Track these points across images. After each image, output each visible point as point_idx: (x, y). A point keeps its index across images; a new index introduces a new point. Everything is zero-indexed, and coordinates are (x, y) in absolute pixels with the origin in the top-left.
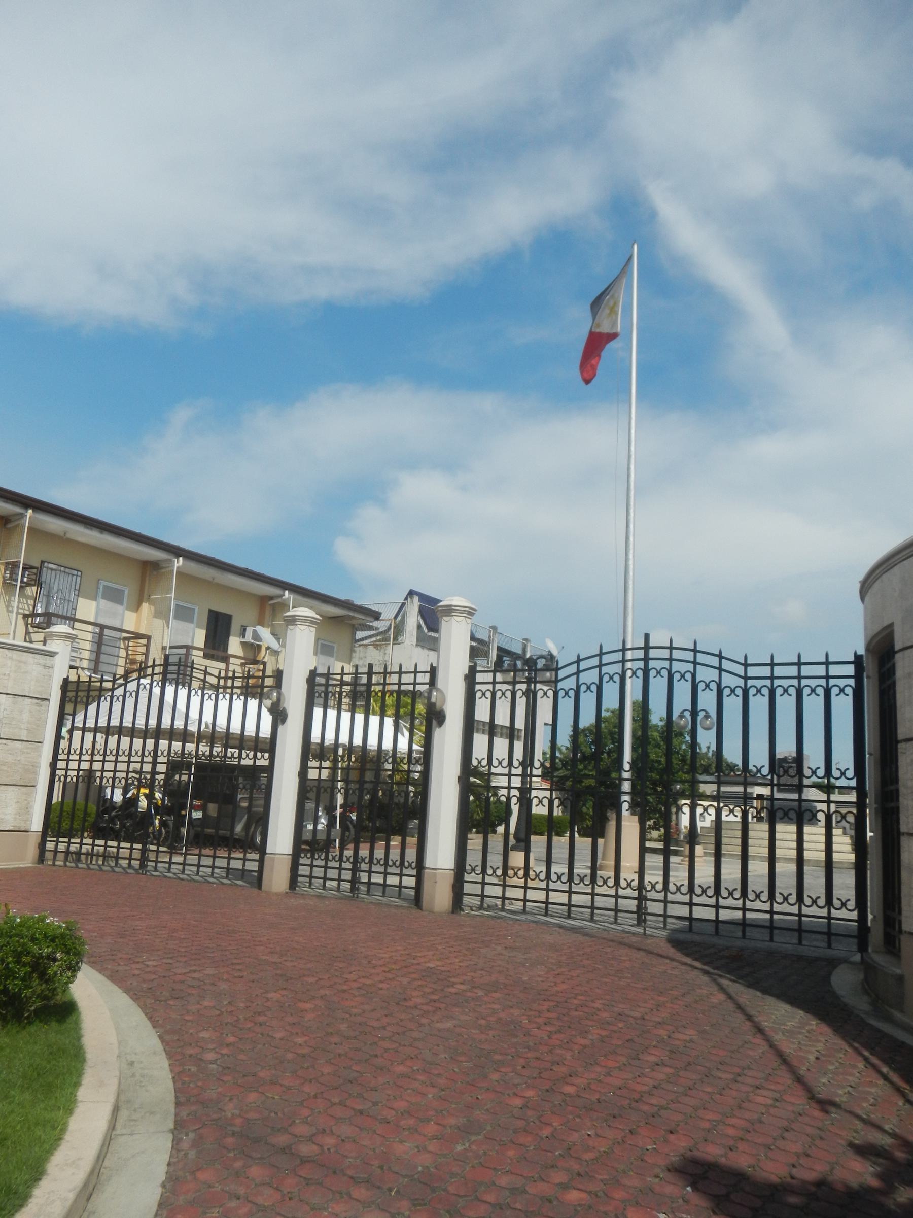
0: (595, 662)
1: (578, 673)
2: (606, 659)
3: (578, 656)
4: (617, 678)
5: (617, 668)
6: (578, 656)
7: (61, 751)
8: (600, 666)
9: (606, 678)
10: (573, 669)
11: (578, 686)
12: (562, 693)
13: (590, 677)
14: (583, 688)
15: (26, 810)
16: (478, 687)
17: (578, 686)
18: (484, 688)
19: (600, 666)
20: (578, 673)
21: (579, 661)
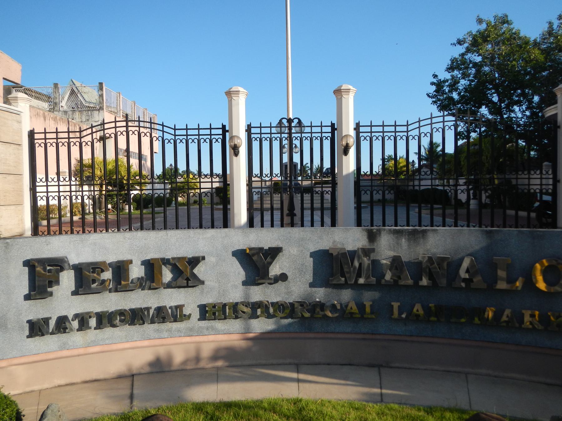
0: (429, 121)
1: (419, 127)
2: (434, 120)
3: (419, 119)
4: (440, 130)
5: (441, 125)
6: (419, 119)
7: (38, 180)
8: (431, 124)
9: (435, 130)
10: (417, 125)
11: (420, 134)
12: (411, 138)
13: (427, 129)
14: (423, 135)
15: (22, 220)
16: (361, 134)
17: (420, 134)
18: (365, 135)
19: (431, 124)
20: (419, 127)
21: (419, 121)
